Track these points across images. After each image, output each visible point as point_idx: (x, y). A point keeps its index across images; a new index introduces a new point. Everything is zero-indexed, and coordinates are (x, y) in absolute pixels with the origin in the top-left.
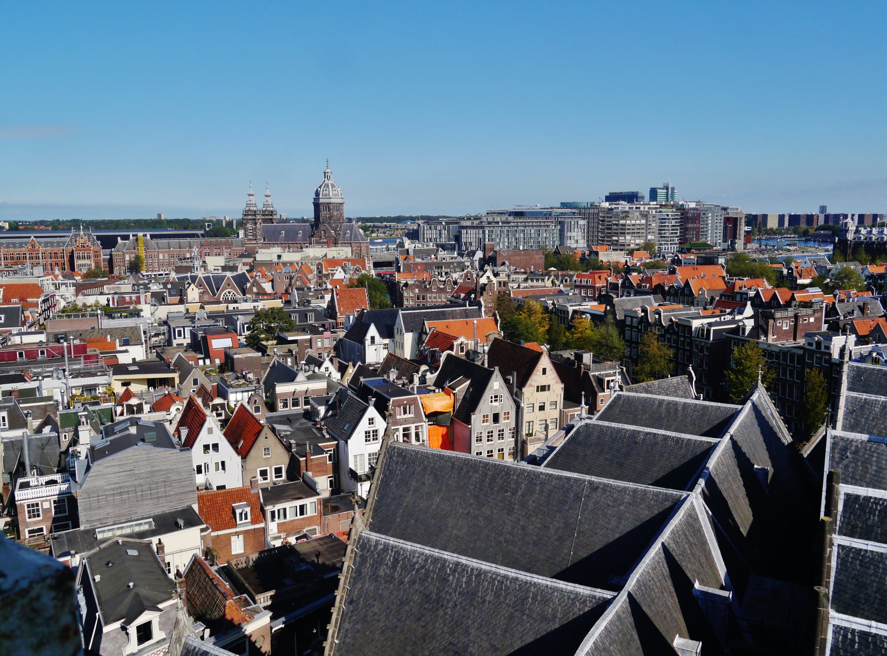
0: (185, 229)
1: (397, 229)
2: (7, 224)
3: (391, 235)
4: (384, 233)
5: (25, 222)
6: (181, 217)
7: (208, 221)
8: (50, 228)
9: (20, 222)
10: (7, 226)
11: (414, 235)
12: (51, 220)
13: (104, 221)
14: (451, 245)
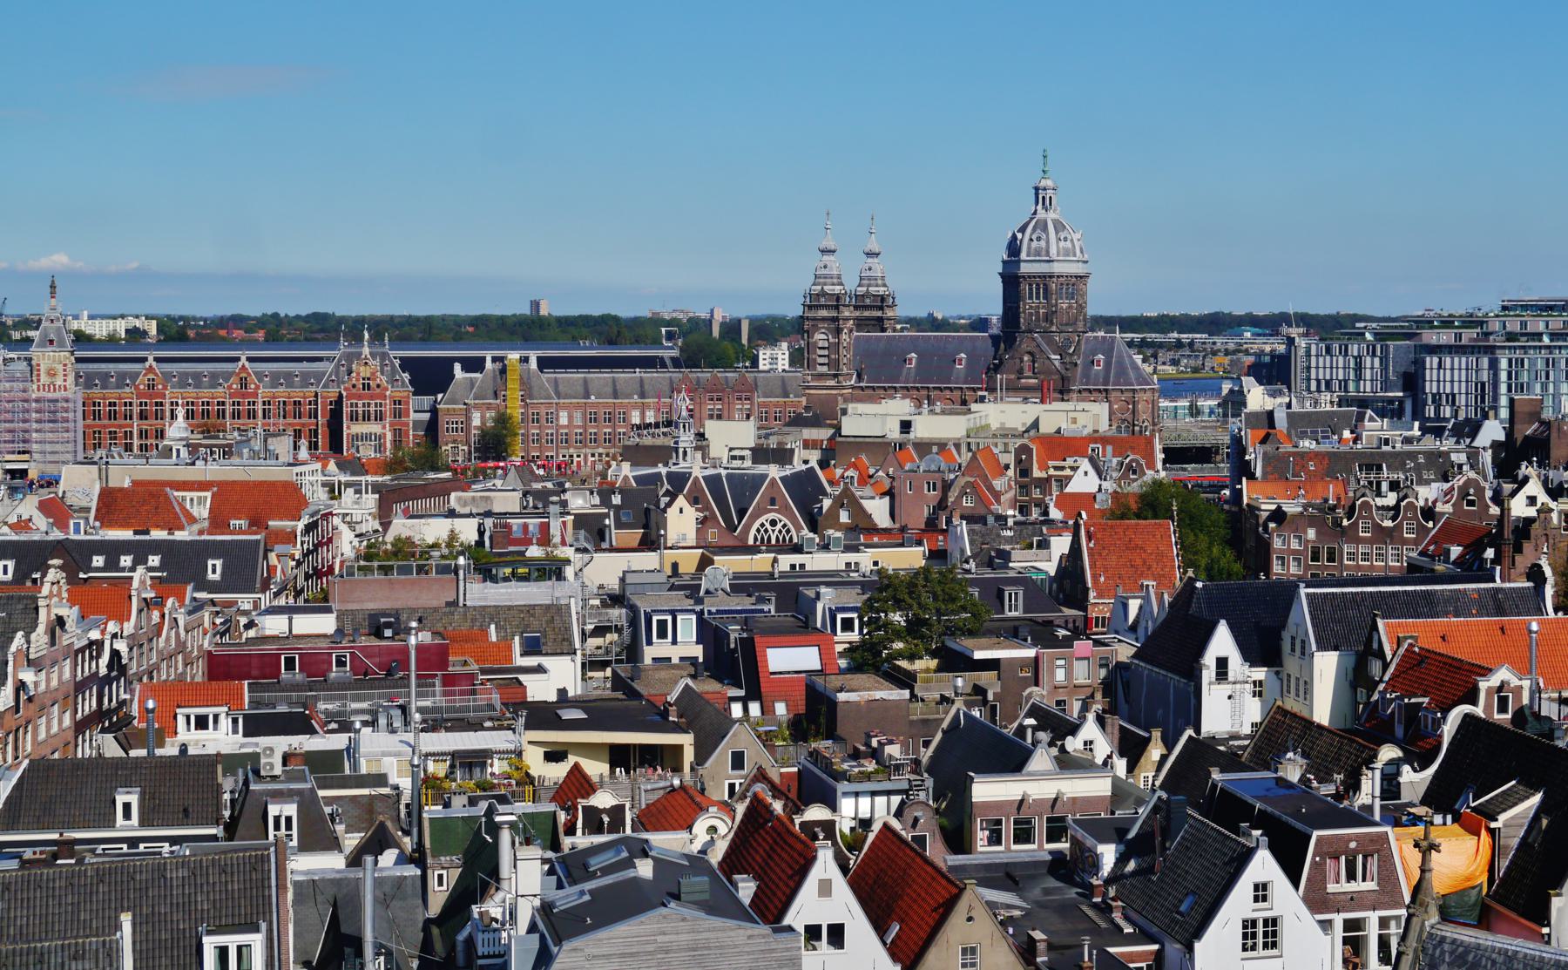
0: (612, 342)
1: (1214, 353)
3: (1196, 370)
4: (1175, 362)
5: (194, 319)
6: (594, 309)
7: (668, 323)
8: (260, 335)
9: (181, 318)
10: (152, 328)
11: (1275, 372)
12: (259, 314)
13: (392, 318)
14: (1391, 401)
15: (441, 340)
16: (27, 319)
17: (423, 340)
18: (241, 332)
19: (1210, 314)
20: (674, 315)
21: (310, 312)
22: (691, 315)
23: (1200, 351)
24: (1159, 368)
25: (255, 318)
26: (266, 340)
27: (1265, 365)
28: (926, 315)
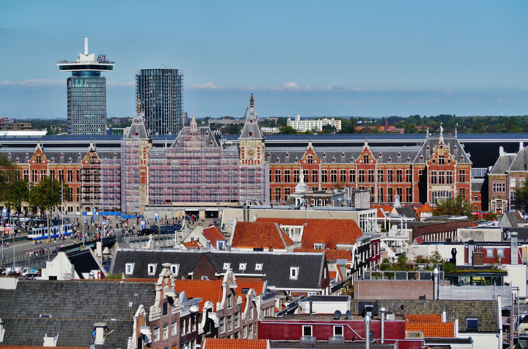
2: (340, 122)
5: (368, 119)
9: (360, 119)
13: (489, 118)
15: (516, 132)
16: (267, 120)
17: (503, 132)
18: (394, 127)
21: (439, 115)
25: (405, 119)
26: (405, 132)
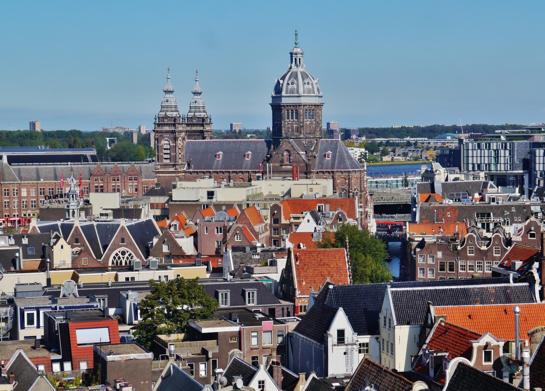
0: (71, 147)
1: (428, 149)
3: (416, 159)
4: (405, 155)
6: (67, 128)
7: (112, 135)
14: (516, 176)
19: (431, 126)
20: (117, 130)
22: (127, 130)
23: (420, 148)
24: (395, 158)
27: (446, 156)
28: (266, 129)
